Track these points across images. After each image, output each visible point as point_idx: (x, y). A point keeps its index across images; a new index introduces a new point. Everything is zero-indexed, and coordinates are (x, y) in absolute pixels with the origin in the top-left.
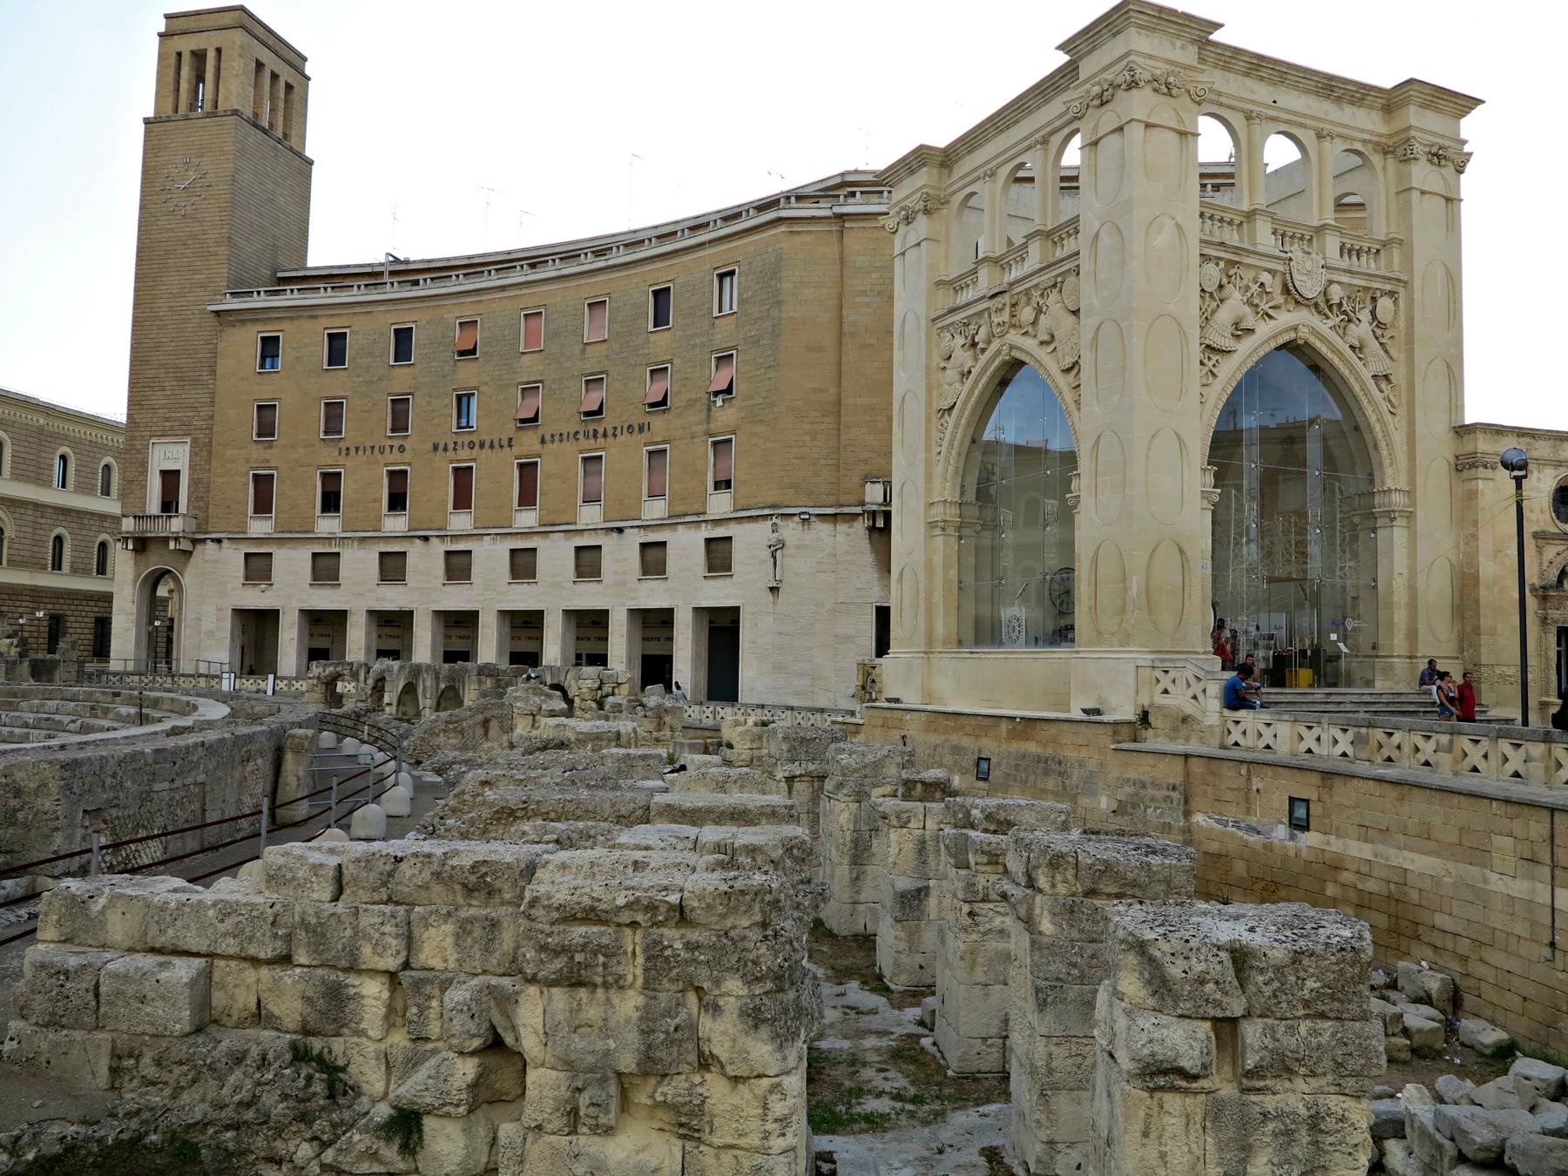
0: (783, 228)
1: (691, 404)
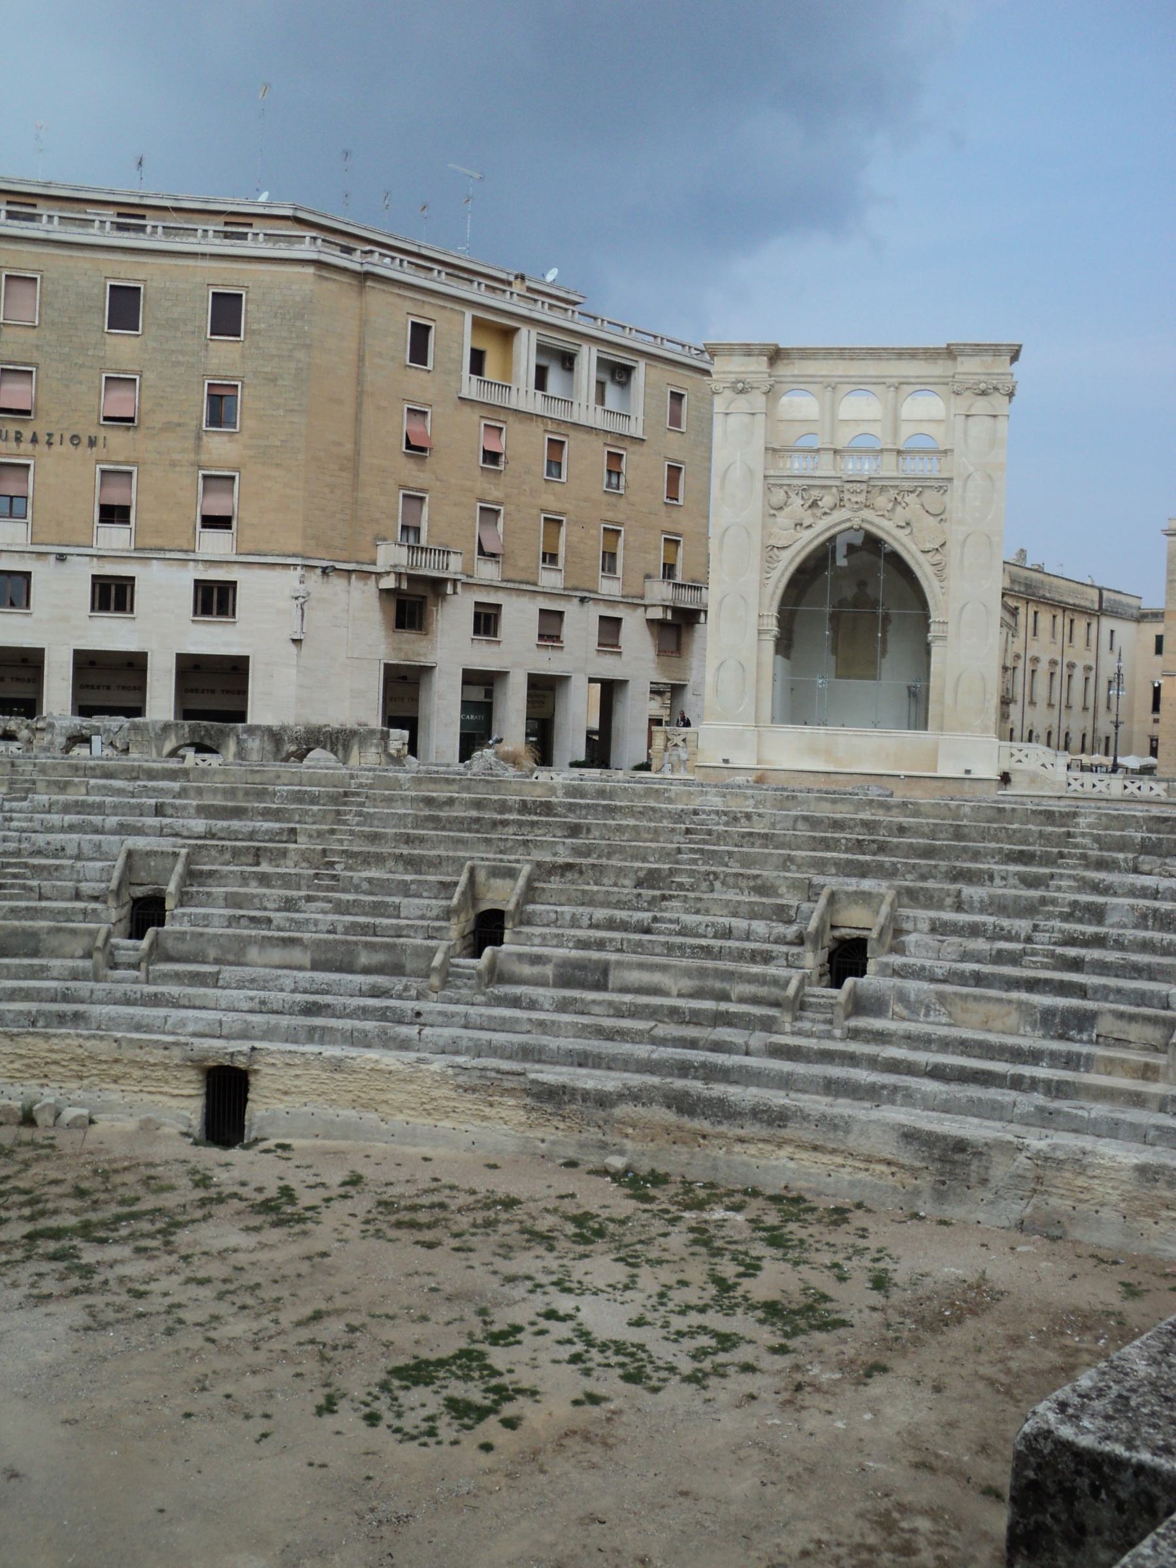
0: (311, 270)
1: (168, 427)
